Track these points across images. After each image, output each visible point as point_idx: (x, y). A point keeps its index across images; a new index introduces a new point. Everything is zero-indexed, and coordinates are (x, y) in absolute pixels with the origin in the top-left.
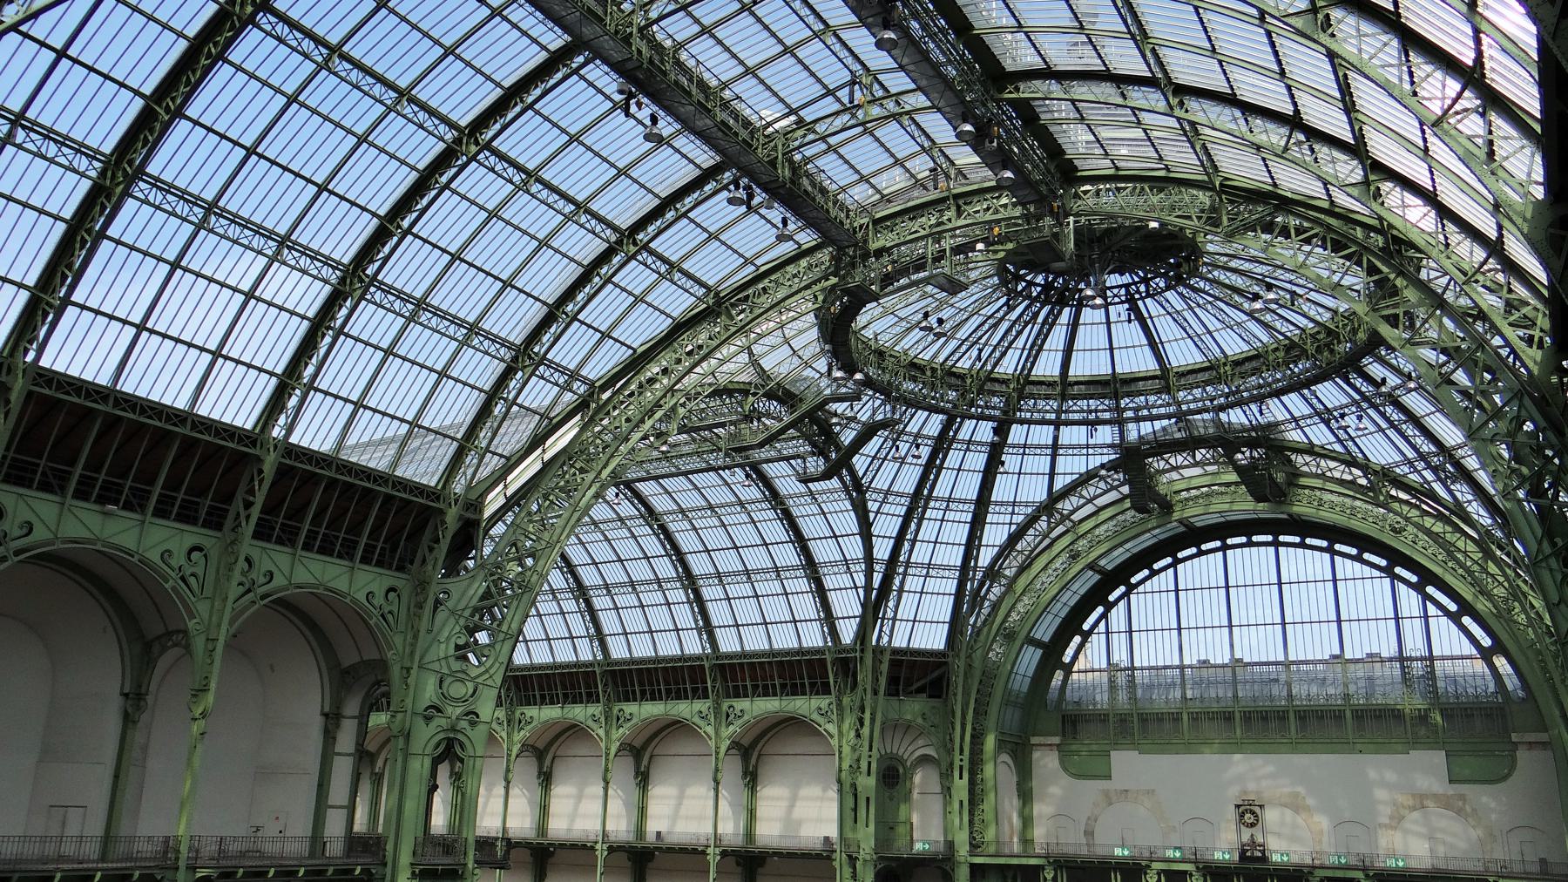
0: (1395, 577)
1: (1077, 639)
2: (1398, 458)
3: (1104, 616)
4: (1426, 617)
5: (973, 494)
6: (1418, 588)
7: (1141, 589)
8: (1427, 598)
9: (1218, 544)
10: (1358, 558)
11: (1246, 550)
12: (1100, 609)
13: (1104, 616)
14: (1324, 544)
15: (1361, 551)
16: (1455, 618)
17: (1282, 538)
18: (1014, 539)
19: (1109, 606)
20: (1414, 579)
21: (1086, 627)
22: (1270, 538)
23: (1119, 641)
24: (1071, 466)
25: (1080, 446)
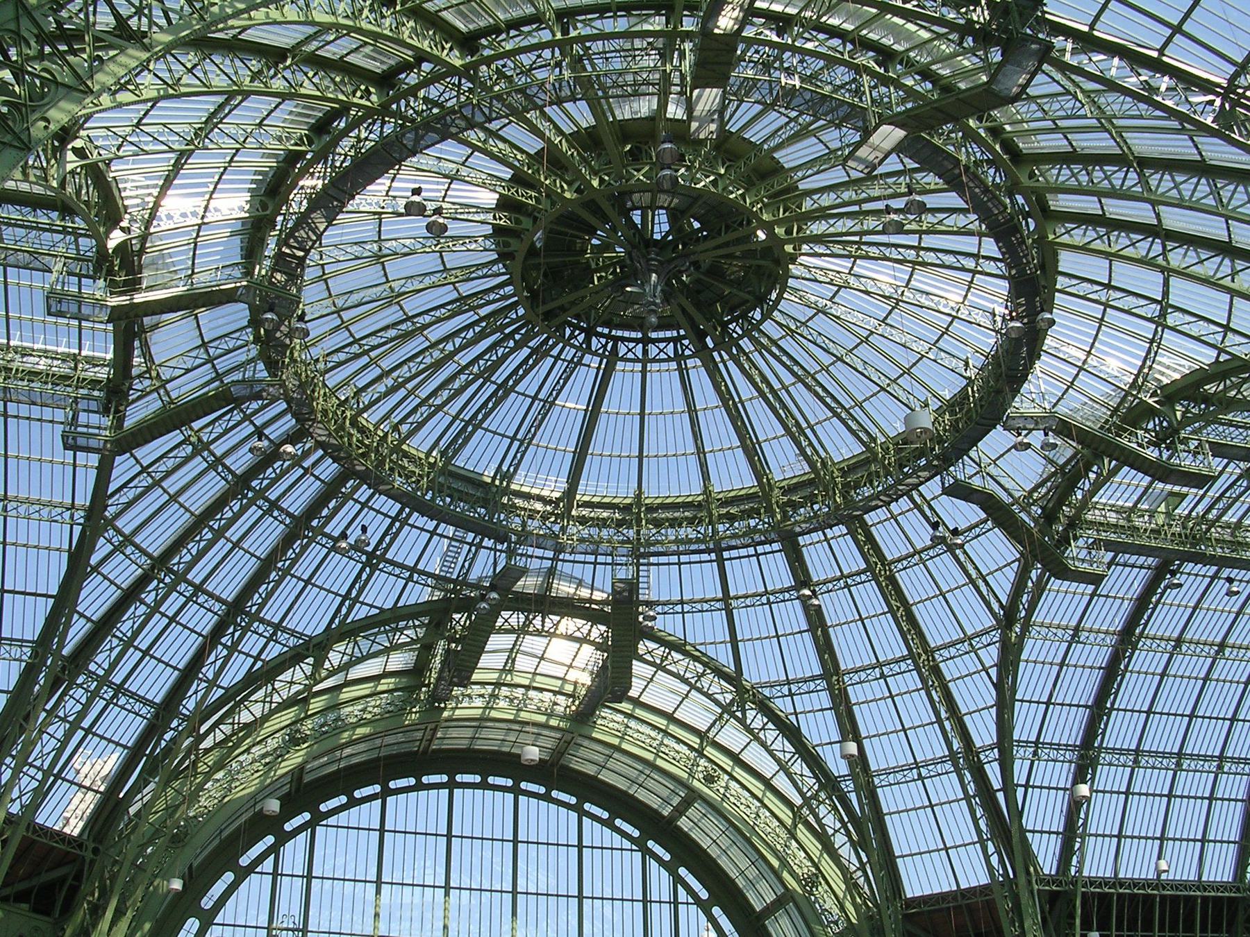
0: (646, 852)
1: (229, 877)
2: (777, 675)
3: (274, 850)
4: (675, 903)
5: (229, 594)
6: (671, 868)
7: (332, 820)
8: (678, 880)
9: (445, 778)
10: (608, 824)
11: (479, 792)
12: (270, 840)
13: (274, 850)
14: (573, 800)
15: (614, 814)
16: (705, 907)
17: (523, 785)
18: (254, 680)
19: (284, 838)
20: (667, 857)
21: (244, 861)
22: (510, 783)
23: (291, 890)
24: (383, 592)
25: (402, 566)
